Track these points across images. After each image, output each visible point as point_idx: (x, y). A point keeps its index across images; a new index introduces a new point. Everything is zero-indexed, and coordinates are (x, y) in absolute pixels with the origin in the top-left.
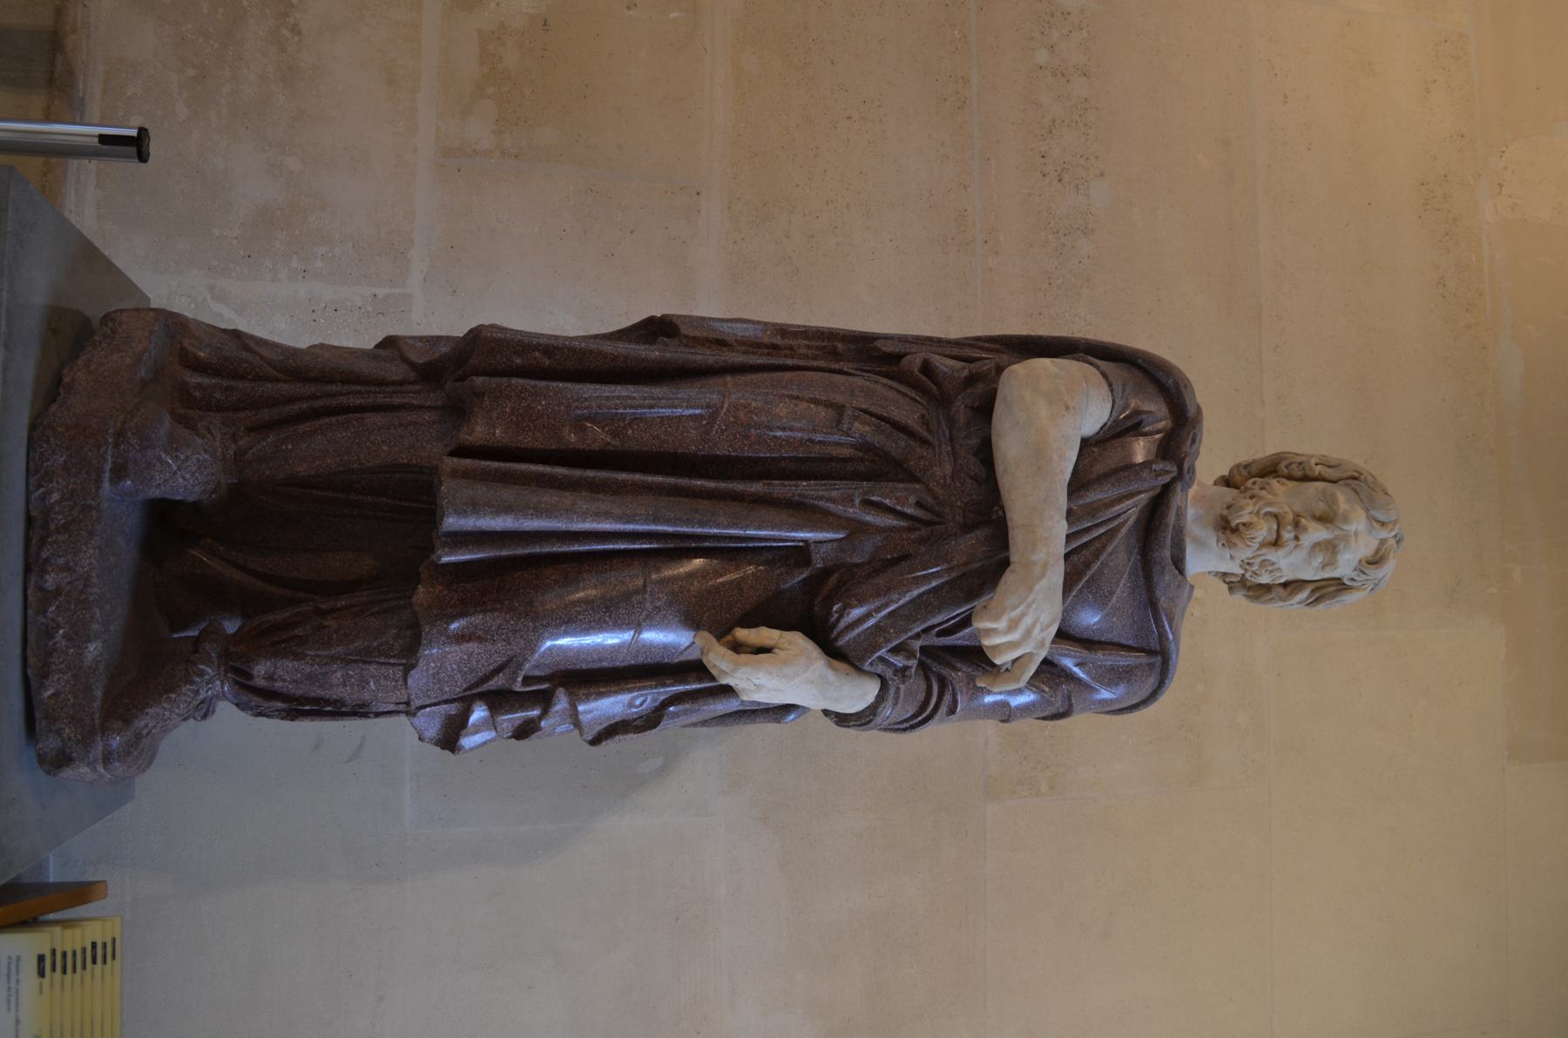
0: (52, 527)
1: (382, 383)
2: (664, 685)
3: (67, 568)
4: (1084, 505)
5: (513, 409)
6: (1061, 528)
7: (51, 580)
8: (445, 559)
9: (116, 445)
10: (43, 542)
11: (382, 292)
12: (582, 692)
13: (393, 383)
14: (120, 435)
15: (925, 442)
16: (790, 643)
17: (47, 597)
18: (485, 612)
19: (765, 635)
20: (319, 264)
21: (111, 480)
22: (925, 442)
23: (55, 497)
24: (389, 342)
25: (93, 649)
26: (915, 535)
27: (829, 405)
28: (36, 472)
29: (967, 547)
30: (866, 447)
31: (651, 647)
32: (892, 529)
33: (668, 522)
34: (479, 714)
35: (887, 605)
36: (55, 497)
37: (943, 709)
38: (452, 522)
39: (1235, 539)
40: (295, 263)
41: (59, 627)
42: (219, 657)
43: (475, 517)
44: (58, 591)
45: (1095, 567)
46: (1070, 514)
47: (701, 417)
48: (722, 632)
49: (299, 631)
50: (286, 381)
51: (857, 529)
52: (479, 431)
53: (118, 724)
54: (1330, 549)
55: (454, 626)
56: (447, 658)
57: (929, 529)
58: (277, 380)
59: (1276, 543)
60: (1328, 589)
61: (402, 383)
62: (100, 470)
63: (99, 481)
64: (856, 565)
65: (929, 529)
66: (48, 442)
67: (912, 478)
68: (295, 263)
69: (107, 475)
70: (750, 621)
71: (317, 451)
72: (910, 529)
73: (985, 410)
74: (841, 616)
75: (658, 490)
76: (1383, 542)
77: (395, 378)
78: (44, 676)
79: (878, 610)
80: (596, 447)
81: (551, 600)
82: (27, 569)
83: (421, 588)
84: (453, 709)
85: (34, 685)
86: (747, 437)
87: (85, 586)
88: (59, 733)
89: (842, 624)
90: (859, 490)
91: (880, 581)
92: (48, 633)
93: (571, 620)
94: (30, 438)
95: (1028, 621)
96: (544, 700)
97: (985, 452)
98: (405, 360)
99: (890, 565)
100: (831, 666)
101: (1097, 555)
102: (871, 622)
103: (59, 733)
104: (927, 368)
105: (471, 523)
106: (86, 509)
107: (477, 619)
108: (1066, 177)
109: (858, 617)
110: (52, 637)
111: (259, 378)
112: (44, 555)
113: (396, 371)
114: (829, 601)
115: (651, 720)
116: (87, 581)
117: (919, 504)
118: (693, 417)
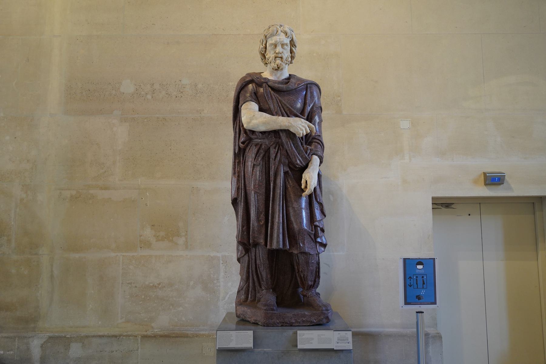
1: (249, 261)
3: (291, 318)
6: (281, 118)
11: (221, 262)
15: (261, 145)
19: (303, 181)
24: (239, 260)
29: (283, 137)
31: (306, 205)
32: (280, 154)
34: (319, 240)
37: (319, 138)
38: (281, 246)
39: (280, 68)
40: (215, 282)
45: (288, 106)
48: (303, 191)
51: (280, 161)
52: (262, 241)
54: (283, 45)
56: (307, 246)
59: (282, 58)
60: (292, 44)
61: (249, 257)
65: (280, 145)
68: (215, 282)
70: (300, 185)
71: (264, 273)
73: (253, 132)
76: (281, 31)
78: (312, 322)
83: (294, 252)
92: (303, 321)
93: (301, 223)
95: (301, 126)
96: (316, 227)
97: (263, 133)
98: (243, 256)
101: (285, 105)
104: (243, 143)
105: (281, 243)
106: (280, 315)
108: (181, 91)
109: (299, 162)
111: (249, 286)
113: (246, 258)
114: (296, 167)
115: (321, 205)
117: (275, 148)
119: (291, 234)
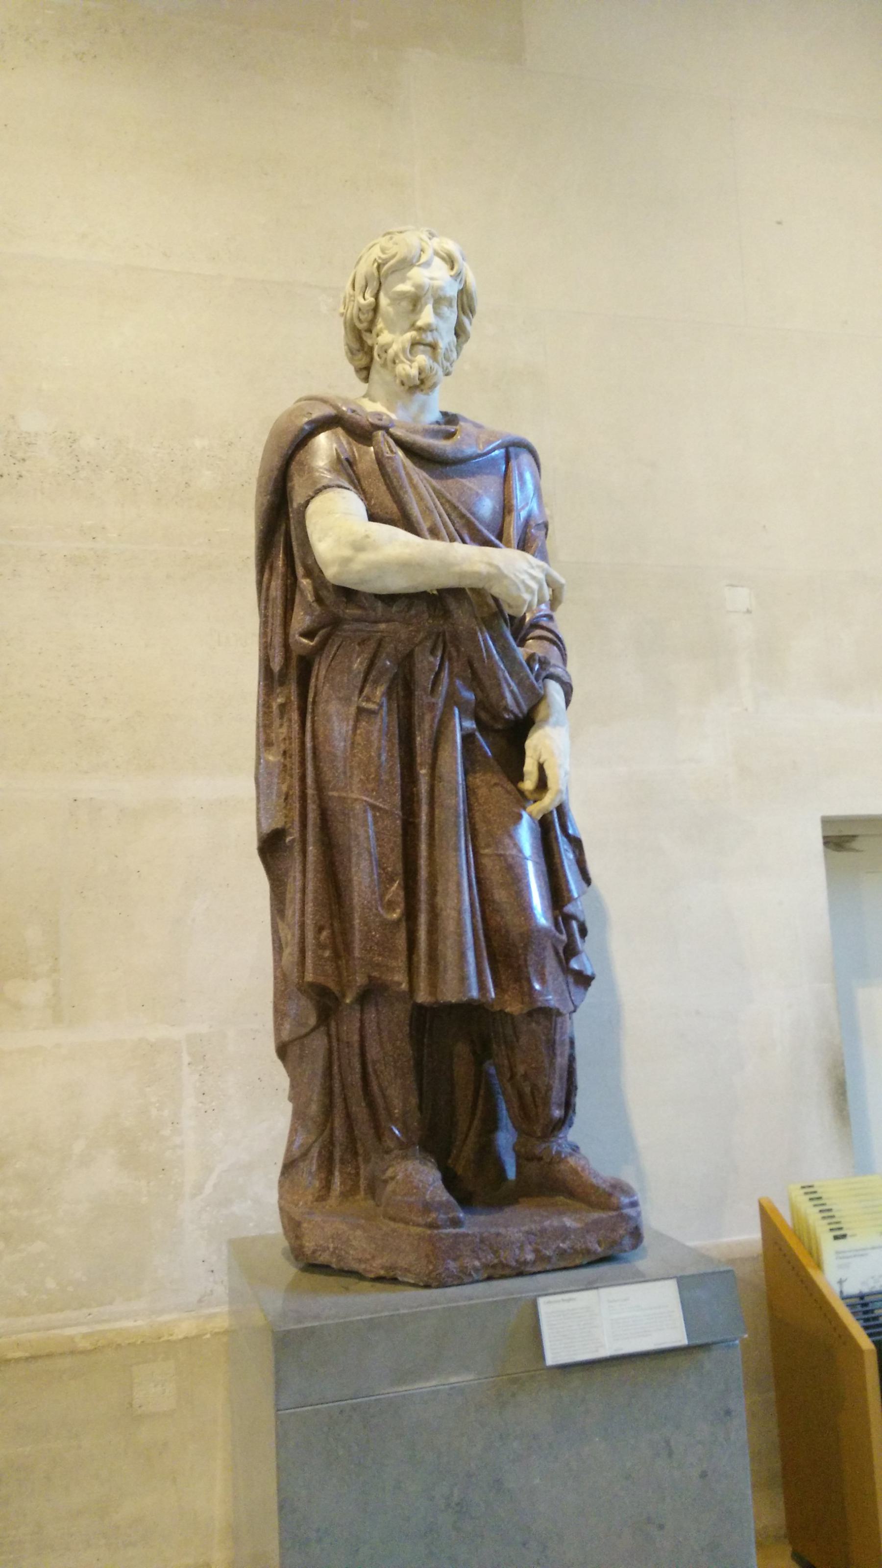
0: (496, 1261)
1: (330, 1051)
2: (556, 838)
3: (521, 1248)
4: (423, 518)
5: (379, 955)
6: (458, 546)
7: (530, 1257)
8: (493, 995)
9: (437, 1227)
10: (504, 1266)
11: (186, 1059)
12: (565, 894)
13: (330, 1042)
14: (432, 1226)
15: (380, 644)
16: (535, 750)
17: (540, 1258)
18: (527, 966)
19: (530, 767)
20: (166, 1113)
21: (461, 1227)
22: (380, 644)
23: (477, 1263)
24: (282, 1051)
25: (569, 1222)
26: (455, 654)
27: (357, 720)
28: (461, 1279)
29: (462, 617)
30: (389, 693)
31: (533, 847)
32: (451, 673)
33: (459, 841)
34: (574, 965)
35: (506, 679)
36: (477, 1263)
37: (550, 625)
38: (475, 993)
39: (429, 383)
40: (166, 1132)
41: (558, 1247)
42: (545, 1142)
43: (466, 978)
44: (536, 1251)
45: (464, 511)
46: (452, 540)
47: (374, 816)
48: (523, 799)
49: (527, 1090)
50: (332, 1123)
51: (452, 699)
52: (400, 978)
53: (614, 1200)
54: (439, 301)
55: (537, 987)
56: (548, 990)
57: (448, 643)
58: (332, 1129)
59: (433, 347)
60: (466, 303)
61: (329, 1035)
62: (456, 1236)
63: (466, 1235)
64: (476, 698)
65: (448, 643)
66: (440, 1274)
67: (410, 656)
68: (166, 1132)
69: (457, 1230)
70: (519, 776)
71: (398, 1093)
72: (450, 659)
73: (347, 594)
74: (512, 712)
75: (431, 846)
76: (436, 253)
77: (326, 1041)
78: (588, 1252)
79: (509, 685)
80: (402, 893)
81: (511, 919)
82: (520, 1274)
83: (508, 1010)
84: (571, 980)
85: (593, 1258)
86: (387, 783)
87: (533, 1234)
88: (622, 1237)
89: (516, 710)
90: (421, 697)
91: (487, 683)
92: (562, 1253)
93: (525, 908)
94: (438, 1287)
95: (525, 577)
96: (568, 918)
97: (390, 599)
98: (306, 1035)
99: (476, 675)
100: (545, 720)
101: (455, 508)
102: (515, 689)
103: (622, 1237)
104: (309, 634)
105: (473, 980)
106: (482, 1241)
107: (531, 970)
108: (20, 455)
109: (511, 697)
110: (565, 1251)
111: (332, 1143)
112: (514, 1264)
113: (319, 1042)
114: (496, 717)
115: (576, 843)
116: (529, 1233)
117: (433, 652)
118: (375, 822)
119: (505, 950)
